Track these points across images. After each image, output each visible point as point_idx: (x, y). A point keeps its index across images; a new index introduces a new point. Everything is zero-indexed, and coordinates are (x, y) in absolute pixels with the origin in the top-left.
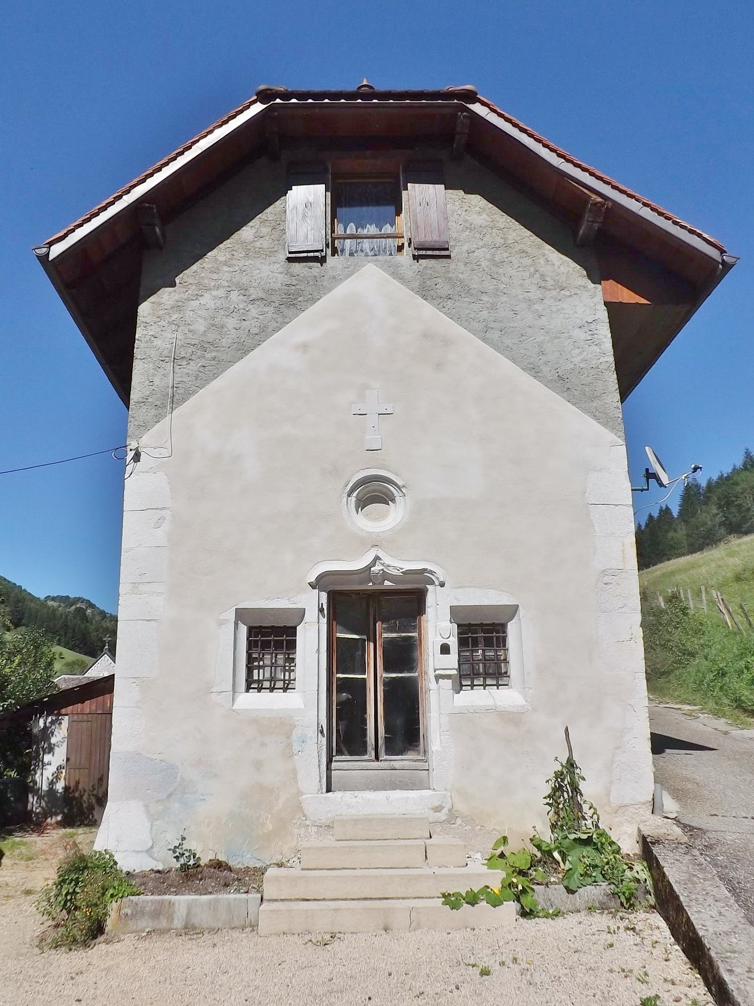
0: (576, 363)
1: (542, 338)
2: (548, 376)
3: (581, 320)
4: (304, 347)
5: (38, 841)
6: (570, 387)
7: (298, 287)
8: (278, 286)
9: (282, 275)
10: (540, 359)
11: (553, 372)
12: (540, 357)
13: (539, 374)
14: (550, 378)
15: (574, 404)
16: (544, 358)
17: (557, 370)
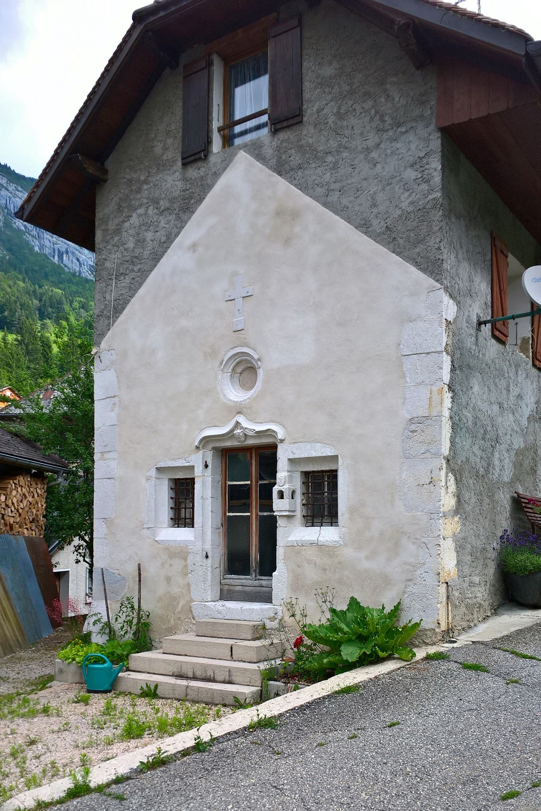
0: (404, 208)
1: (375, 188)
2: (378, 229)
3: (414, 156)
4: (194, 247)
5: (15, 767)
6: (396, 236)
7: (191, 190)
8: (176, 194)
9: (180, 182)
10: (372, 212)
11: (383, 223)
12: (372, 211)
13: (370, 229)
14: (379, 231)
15: (398, 254)
16: (375, 211)
17: (386, 221)
